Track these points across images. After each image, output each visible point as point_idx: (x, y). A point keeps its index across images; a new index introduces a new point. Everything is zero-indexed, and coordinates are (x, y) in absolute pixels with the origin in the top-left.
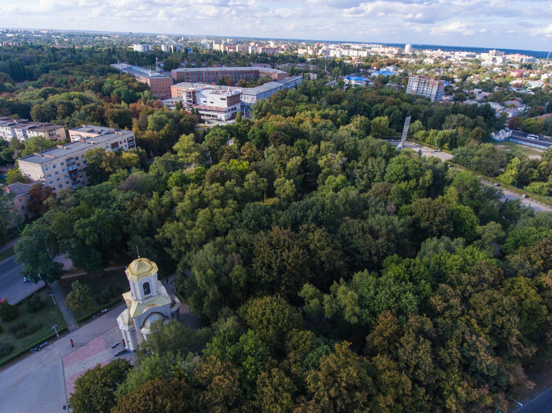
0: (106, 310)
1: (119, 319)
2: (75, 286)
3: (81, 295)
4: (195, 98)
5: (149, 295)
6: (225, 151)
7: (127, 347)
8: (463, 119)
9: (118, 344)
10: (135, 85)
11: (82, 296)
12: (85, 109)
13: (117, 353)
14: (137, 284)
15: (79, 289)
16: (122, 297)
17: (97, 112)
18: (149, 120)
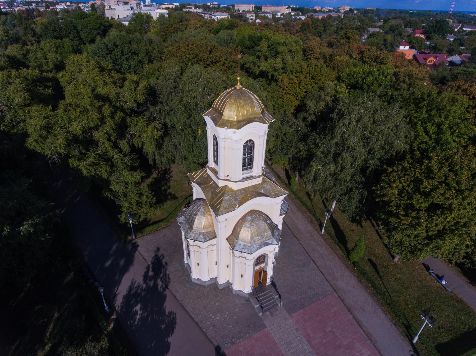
9: (258, 301)
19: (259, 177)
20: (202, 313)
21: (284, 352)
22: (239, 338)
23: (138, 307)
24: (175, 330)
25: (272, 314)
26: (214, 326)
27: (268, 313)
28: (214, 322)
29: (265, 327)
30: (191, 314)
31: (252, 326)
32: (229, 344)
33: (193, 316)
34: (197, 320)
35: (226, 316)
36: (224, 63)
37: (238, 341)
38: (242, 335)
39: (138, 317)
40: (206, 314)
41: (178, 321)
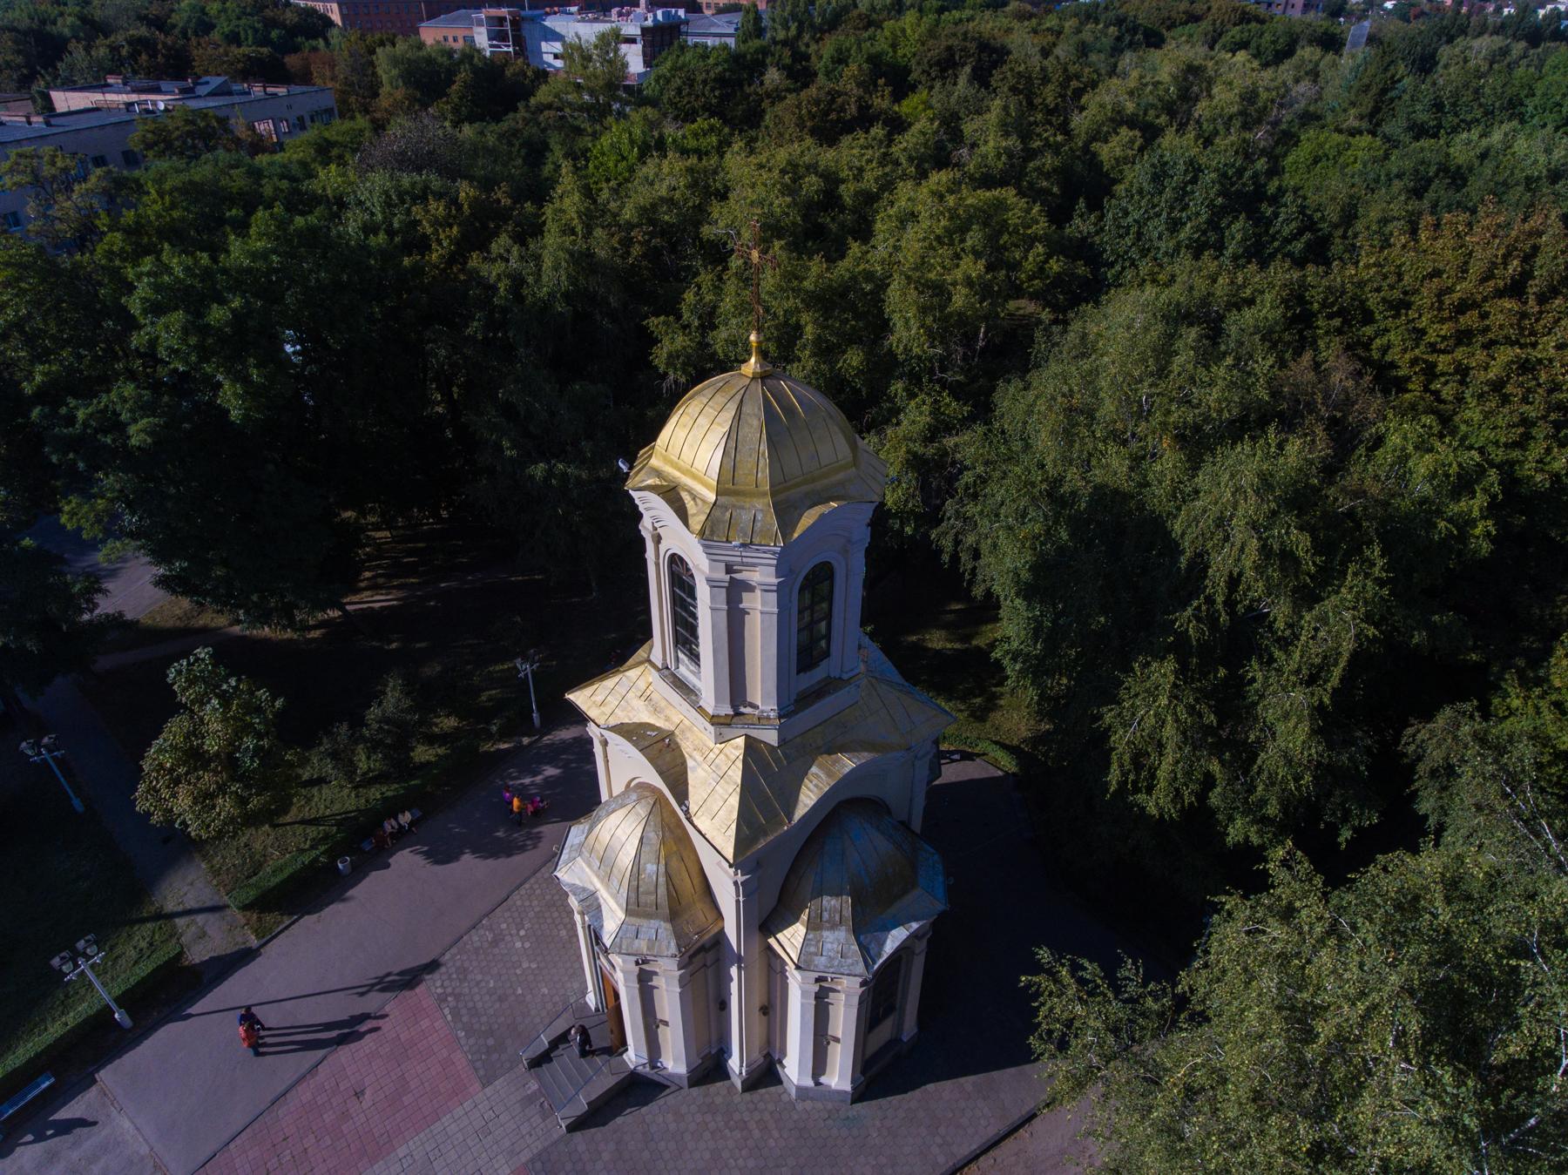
0: (405, 818)
1: (574, 872)
2: (191, 682)
3: (239, 734)
4: (518, 41)
5: (819, 674)
6: (765, 104)
7: (634, 1056)
8: (1504, 52)
10: (290, 17)
11: (249, 742)
12: (114, 49)
13: (582, 1105)
14: (762, 574)
15: (225, 700)
16: (581, 718)
17: (160, 59)
18: (380, 71)
19: (700, 710)
20: (535, 903)
21: (401, 1152)
22: (456, 1013)
23: (551, 771)
24: (490, 861)
25: (529, 1100)
26: (495, 943)
27: (534, 1086)
28: (508, 938)
29: (487, 1082)
30: (532, 880)
31: (491, 1042)
32: (439, 991)
33: (527, 886)
34: (515, 896)
35: (525, 965)
36: (1551, 361)
37: (447, 1011)
38: (465, 1019)
39: (527, 781)
40: (531, 914)
41: (517, 859)
